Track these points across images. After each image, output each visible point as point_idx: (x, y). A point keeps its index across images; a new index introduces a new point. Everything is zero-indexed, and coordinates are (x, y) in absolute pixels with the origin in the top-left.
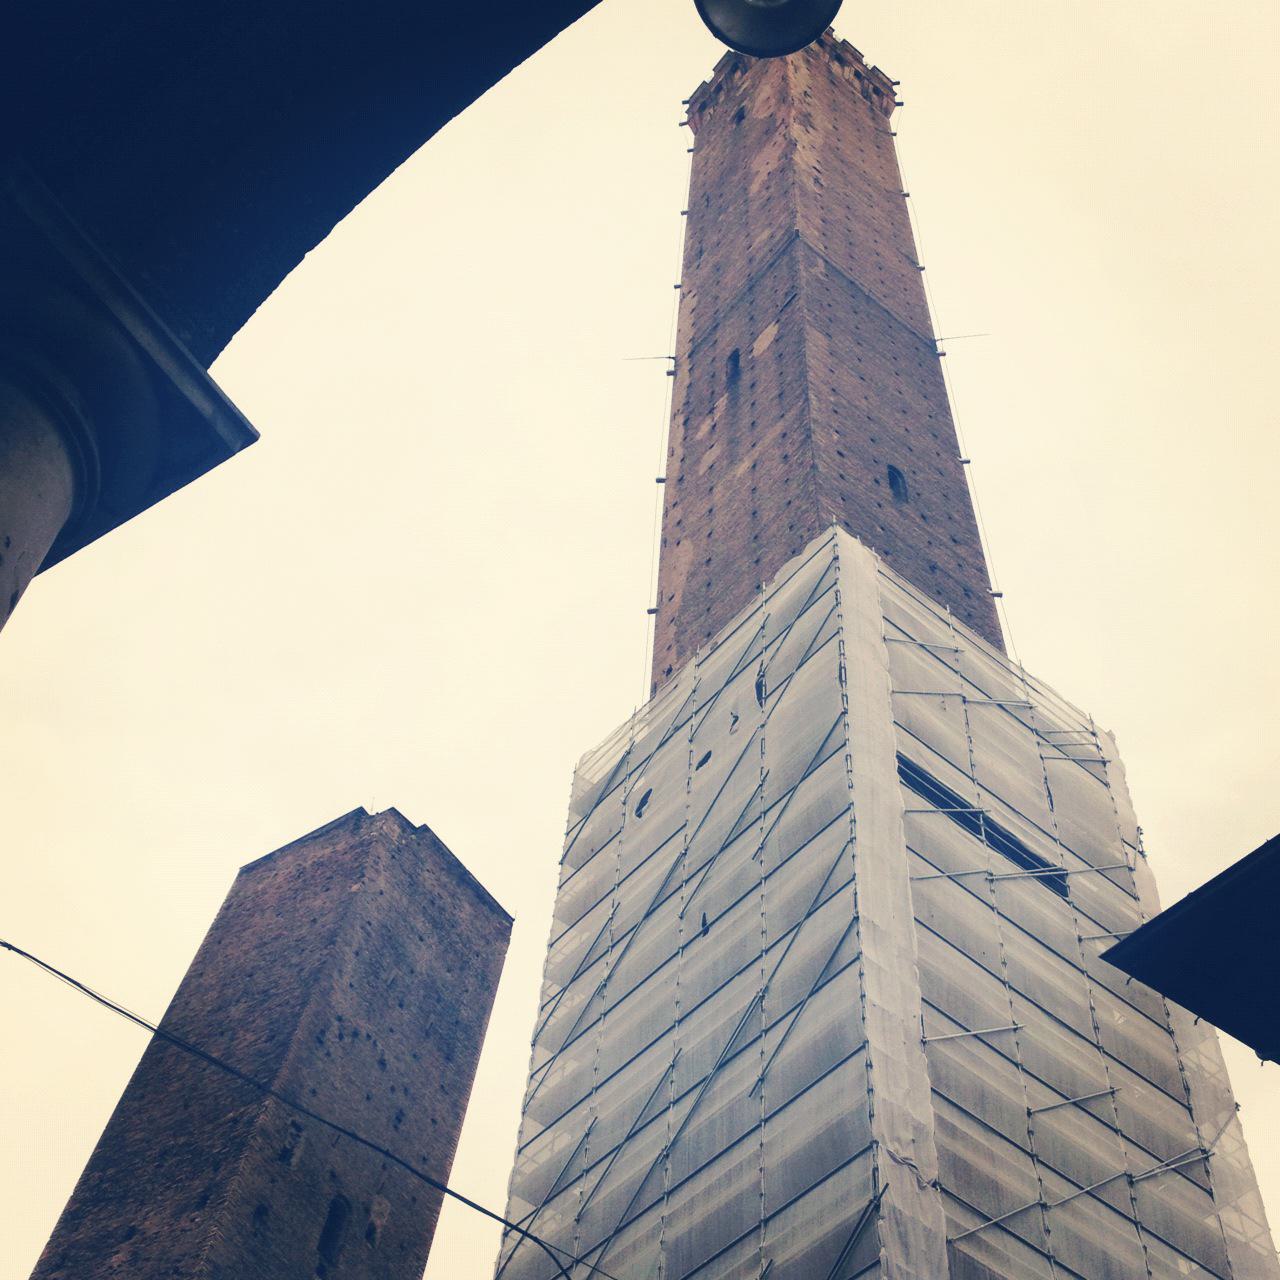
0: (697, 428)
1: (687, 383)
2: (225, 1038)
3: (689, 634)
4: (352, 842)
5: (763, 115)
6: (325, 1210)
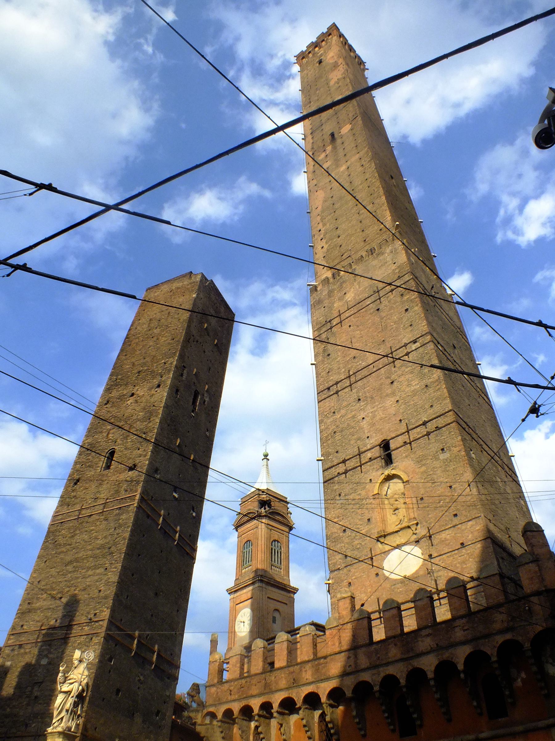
0: (319, 156)
1: (311, 141)
2: (155, 339)
3: (327, 219)
4: (190, 281)
5: (332, 61)
6: (193, 392)
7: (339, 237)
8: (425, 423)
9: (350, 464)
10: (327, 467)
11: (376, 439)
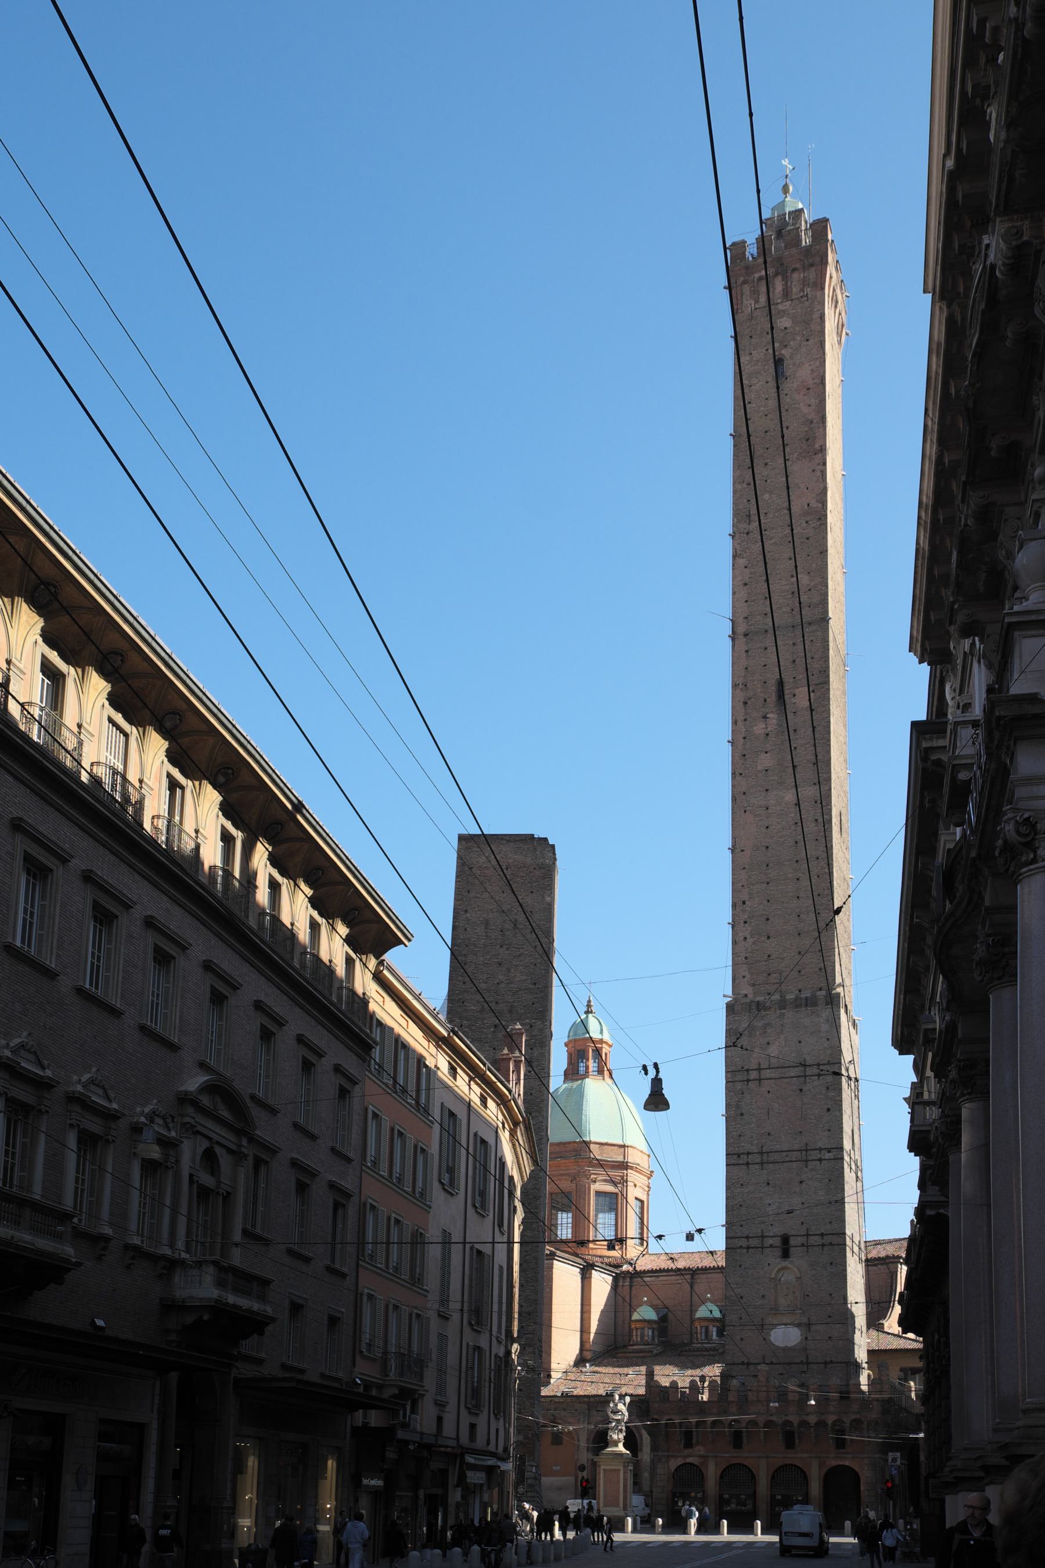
7: (769, 938)
8: (822, 1235)
9: (754, 1242)
10: (732, 1234)
11: (778, 1230)
